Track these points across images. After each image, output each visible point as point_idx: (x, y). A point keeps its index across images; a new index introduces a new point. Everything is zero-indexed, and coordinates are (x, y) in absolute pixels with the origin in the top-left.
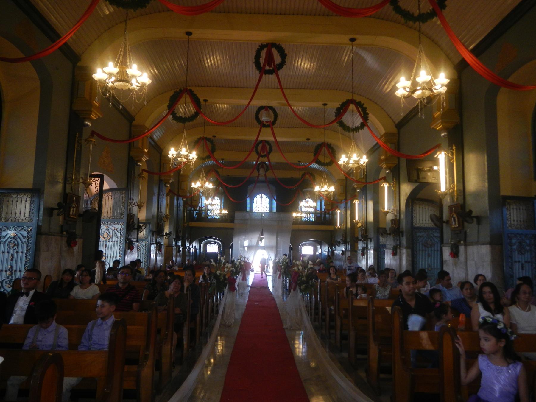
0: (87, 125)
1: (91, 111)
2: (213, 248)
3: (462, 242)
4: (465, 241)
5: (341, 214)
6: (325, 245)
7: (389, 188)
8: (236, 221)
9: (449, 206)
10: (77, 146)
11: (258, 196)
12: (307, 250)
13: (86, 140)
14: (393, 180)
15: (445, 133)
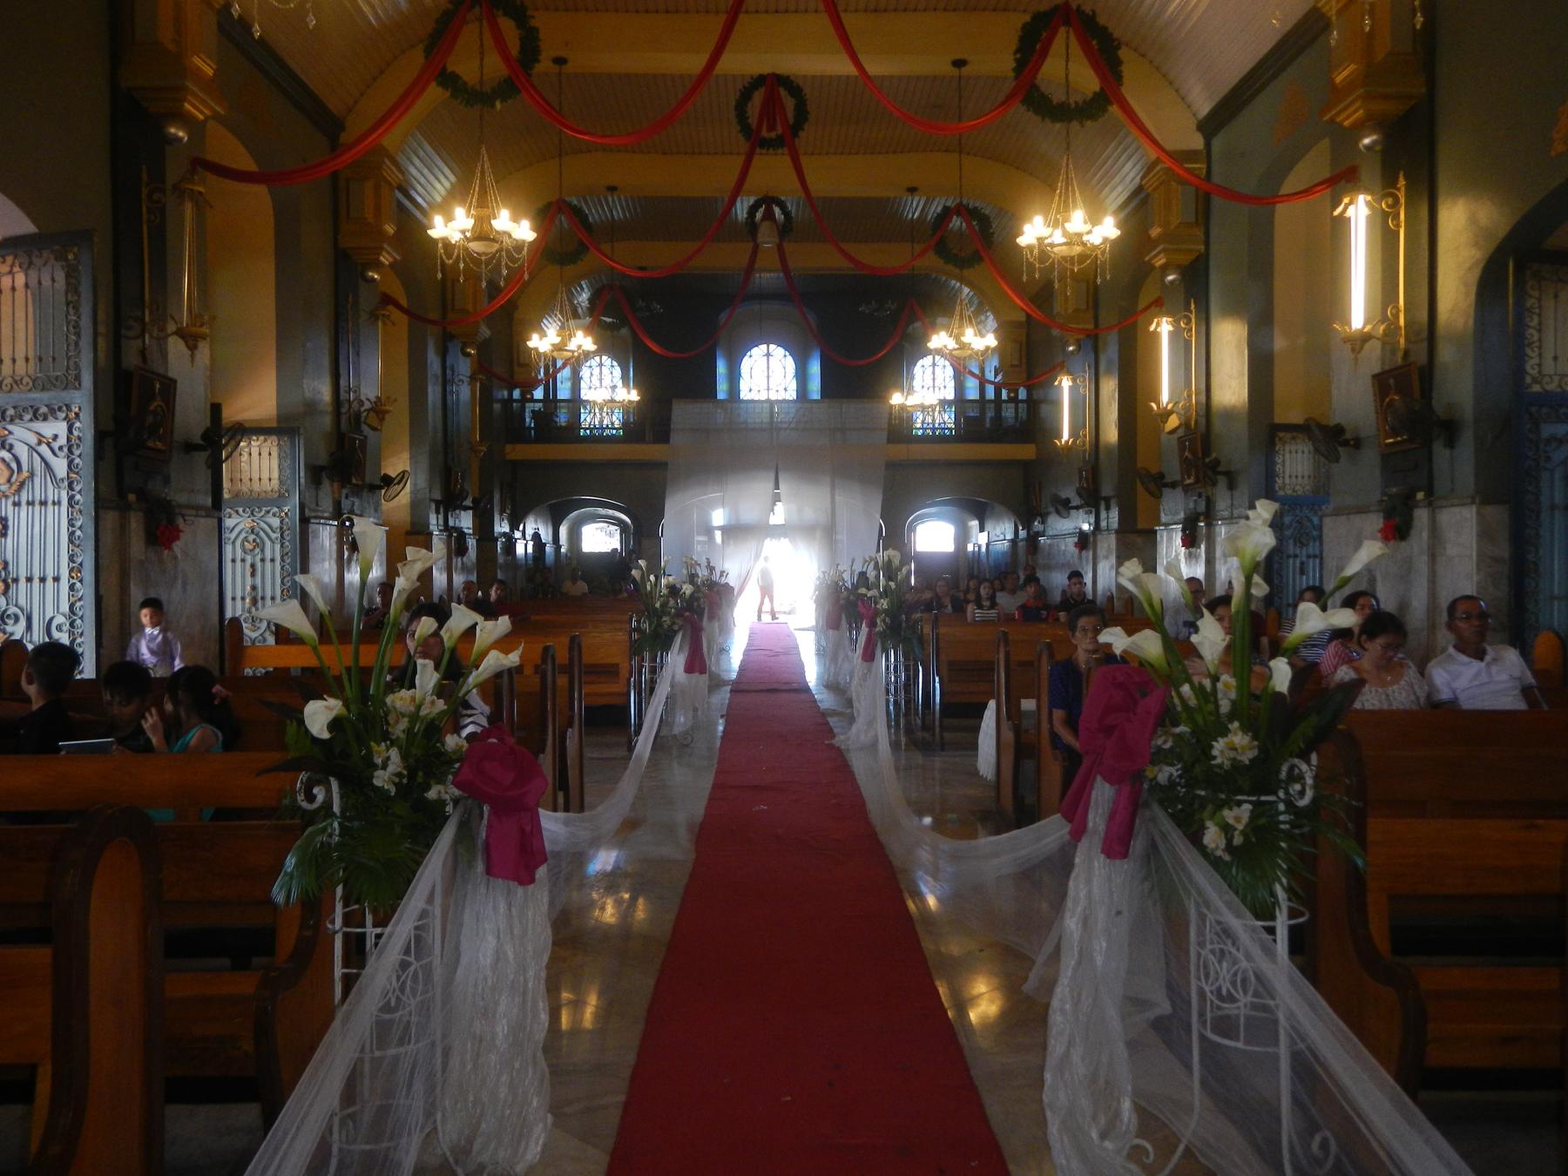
0: (181, 139)
2: (600, 538)
3: (1420, 495)
4: (1430, 493)
6: (998, 518)
7: (1173, 336)
8: (675, 438)
11: (755, 351)
12: (934, 536)
13: (175, 187)
14: (1189, 304)
15: (1375, 137)
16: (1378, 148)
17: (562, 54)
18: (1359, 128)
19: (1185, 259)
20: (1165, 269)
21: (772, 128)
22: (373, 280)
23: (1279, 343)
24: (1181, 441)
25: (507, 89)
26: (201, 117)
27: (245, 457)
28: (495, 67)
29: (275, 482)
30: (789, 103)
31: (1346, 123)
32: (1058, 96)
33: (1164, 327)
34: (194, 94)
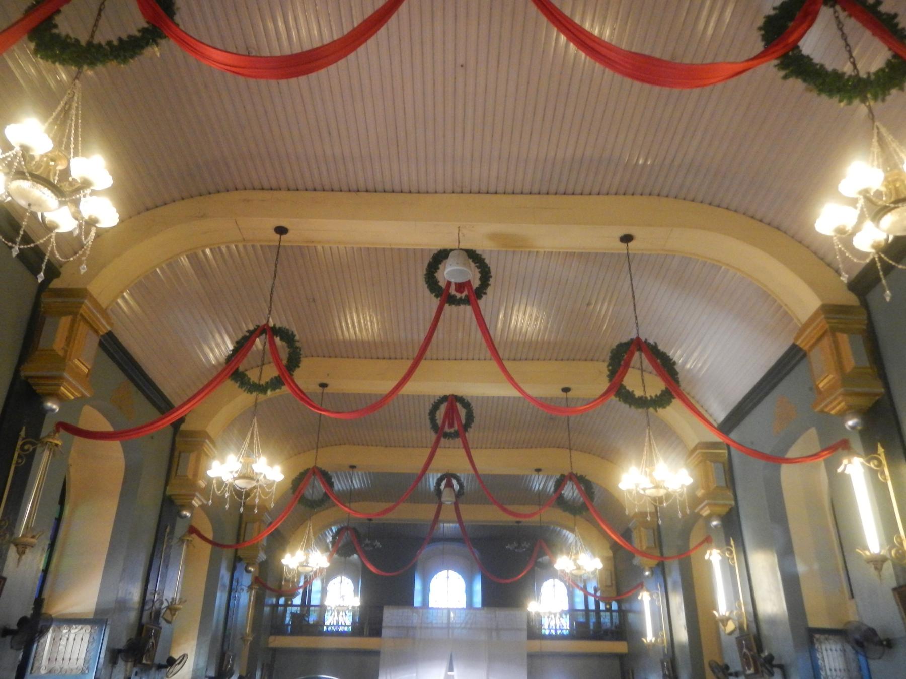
0: (53, 410)
1: (61, 378)
9: (894, 590)
10: (19, 456)
14: (728, 544)
16: (859, 428)
17: (325, 381)
18: (843, 415)
19: (723, 511)
20: (709, 518)
21: (451, 426)
22: (186, 516)
23: (801, 568)
24: (739, 641)
25: (276, 383)
26: (73, 397)
27: (63, 642)
28: (271, 372)
29: (81, 662)
30: (462, 412)
31: (833, 412)
32: (638, 393)
33: (714, 556)
34: (68, 381)
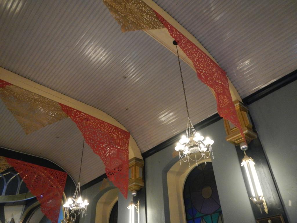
5: (136, 210)
